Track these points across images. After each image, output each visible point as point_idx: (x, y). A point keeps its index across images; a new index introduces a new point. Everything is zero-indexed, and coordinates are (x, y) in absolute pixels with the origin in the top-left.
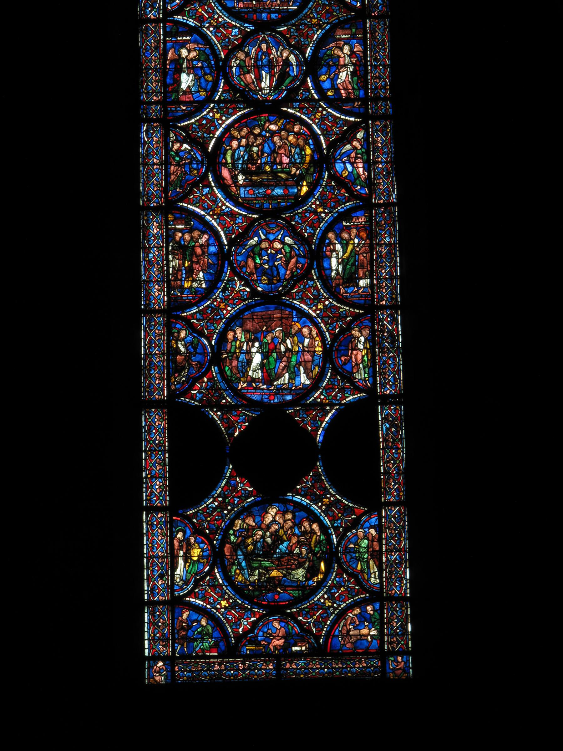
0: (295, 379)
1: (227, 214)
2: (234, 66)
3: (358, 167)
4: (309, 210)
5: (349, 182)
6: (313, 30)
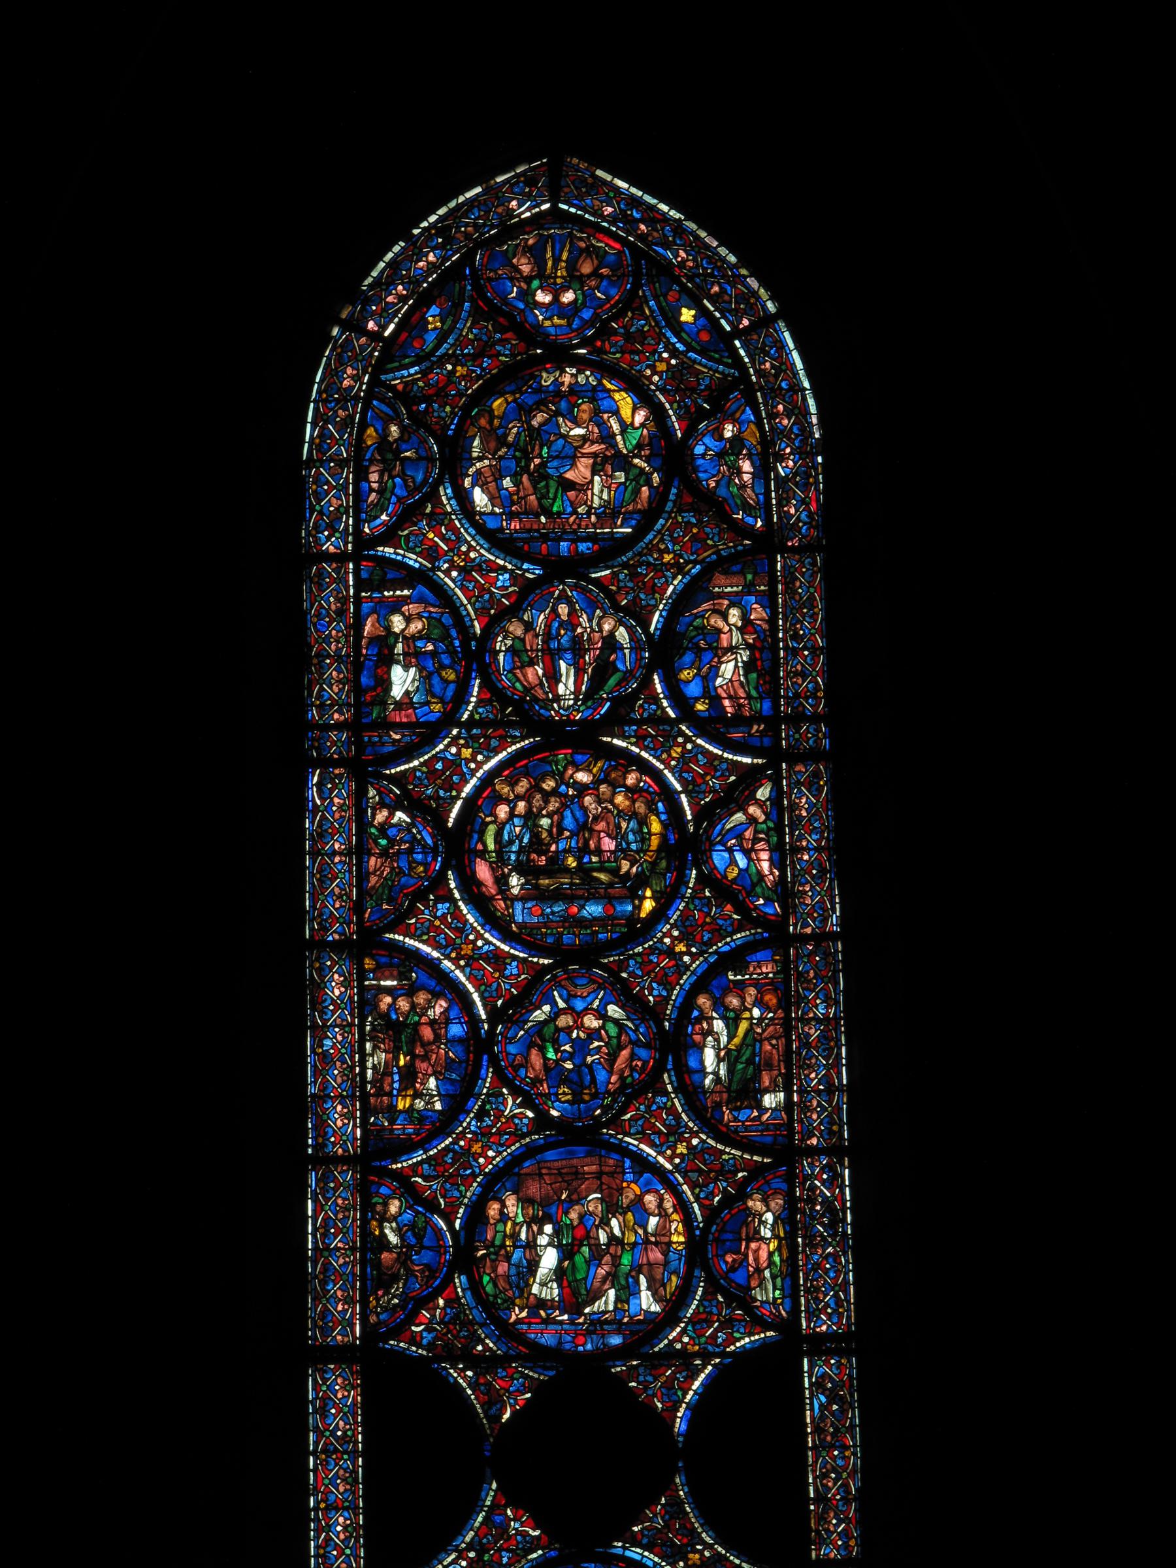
0: (628, 1302)
1: (486, 957)
2: (500, 651)
3: (759, 860)
4: (657, 948)
5: (740, 891)
6: (664, 576)
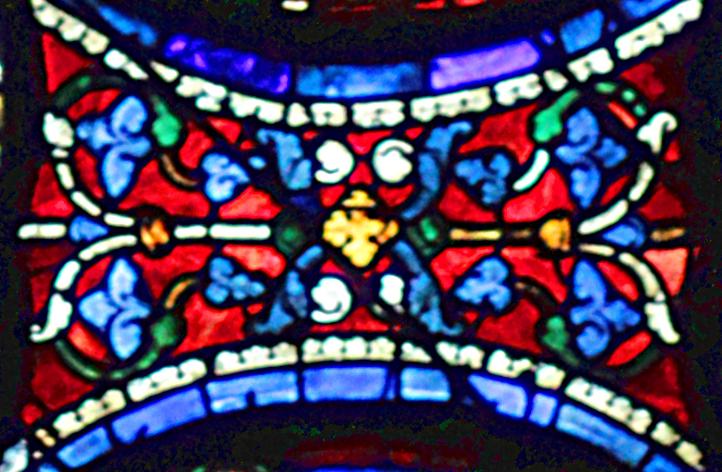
4: (269, 151)
